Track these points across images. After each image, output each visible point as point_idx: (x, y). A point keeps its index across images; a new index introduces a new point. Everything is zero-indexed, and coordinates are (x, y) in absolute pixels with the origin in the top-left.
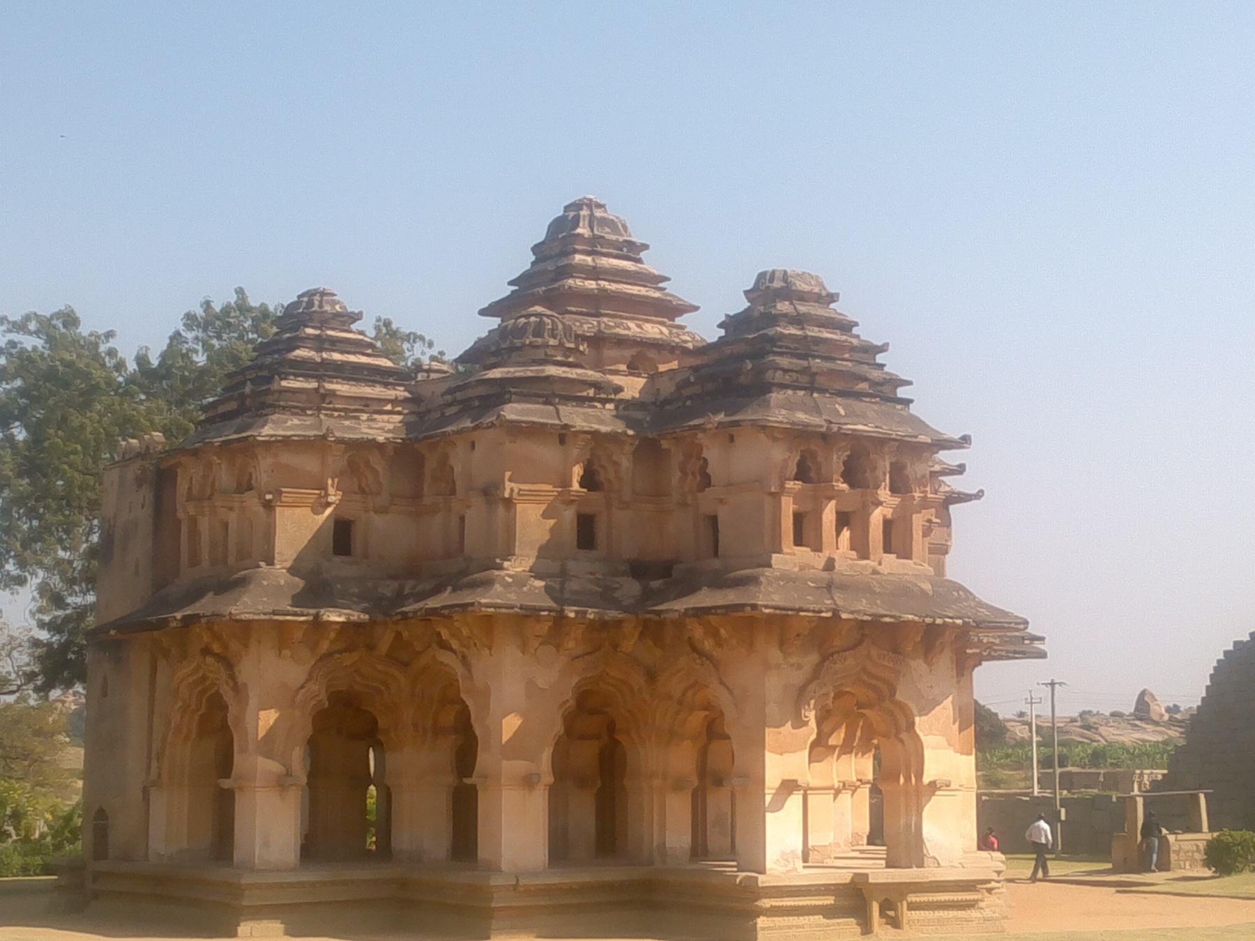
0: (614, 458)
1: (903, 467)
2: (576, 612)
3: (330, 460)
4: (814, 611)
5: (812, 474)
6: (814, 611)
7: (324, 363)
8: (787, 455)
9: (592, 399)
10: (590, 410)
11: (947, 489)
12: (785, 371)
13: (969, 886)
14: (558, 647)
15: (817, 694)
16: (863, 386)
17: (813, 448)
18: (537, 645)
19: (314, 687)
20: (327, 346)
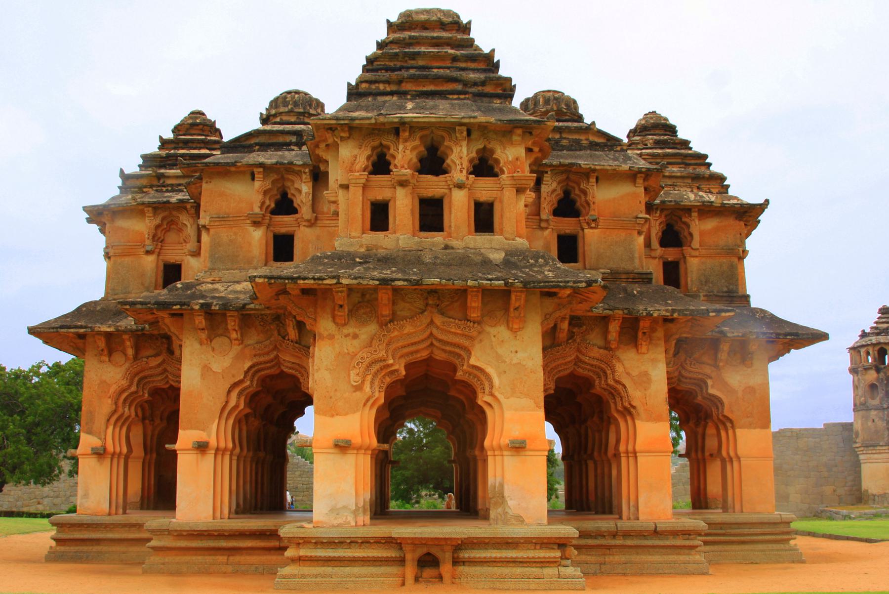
0: (296, 185)
1: (492, 152)
2: (202, 305)
3: (147, 220)
4: (314, 279)
5: (392, 167)
6: (314, 279)
7: (168, 156)
8: (356, 151)
9: (289, 144)
10: (286, 153)
11: (735, 202)
12: (370, 82)
13: (561, 544)
14: (229, 338)
15: (368, 361)
16: (459, 87)
17: (384, 143)
18: (203, 336)
19: (125, 383)
20: (181, 145)
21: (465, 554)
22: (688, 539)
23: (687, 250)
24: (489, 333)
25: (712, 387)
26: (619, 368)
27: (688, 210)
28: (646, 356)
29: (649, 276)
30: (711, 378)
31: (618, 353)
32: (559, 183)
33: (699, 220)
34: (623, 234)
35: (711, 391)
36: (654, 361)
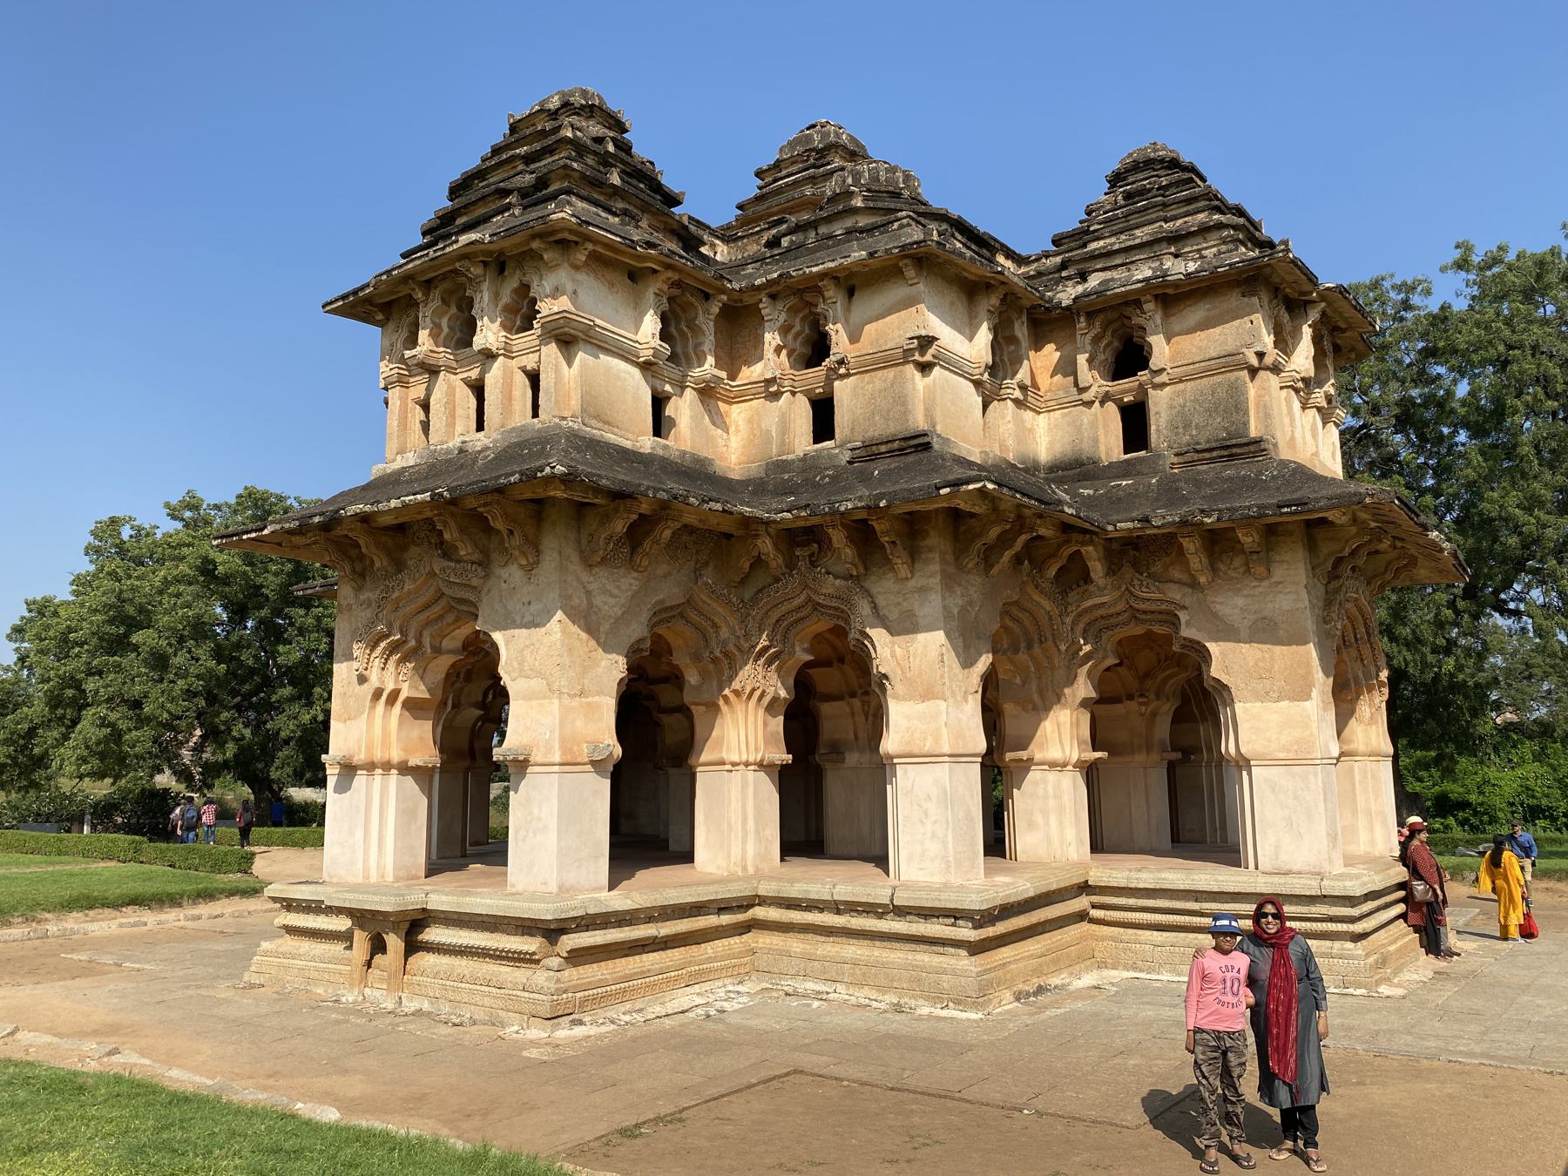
21: (433, 934)
22: (953, 925)
23: (1143, 376)
24: (499, 577)
25: (1188, 623)
26: (864, 608)
27: (1132, 301)
28: (912, 583)
29: (926, 440)
30: (1184, 607)
31: (866, 584)
32: (792, 311)
33: (1166, 316)
34: (890, 374)
35: (1186, 632)
36: (922, 590)
